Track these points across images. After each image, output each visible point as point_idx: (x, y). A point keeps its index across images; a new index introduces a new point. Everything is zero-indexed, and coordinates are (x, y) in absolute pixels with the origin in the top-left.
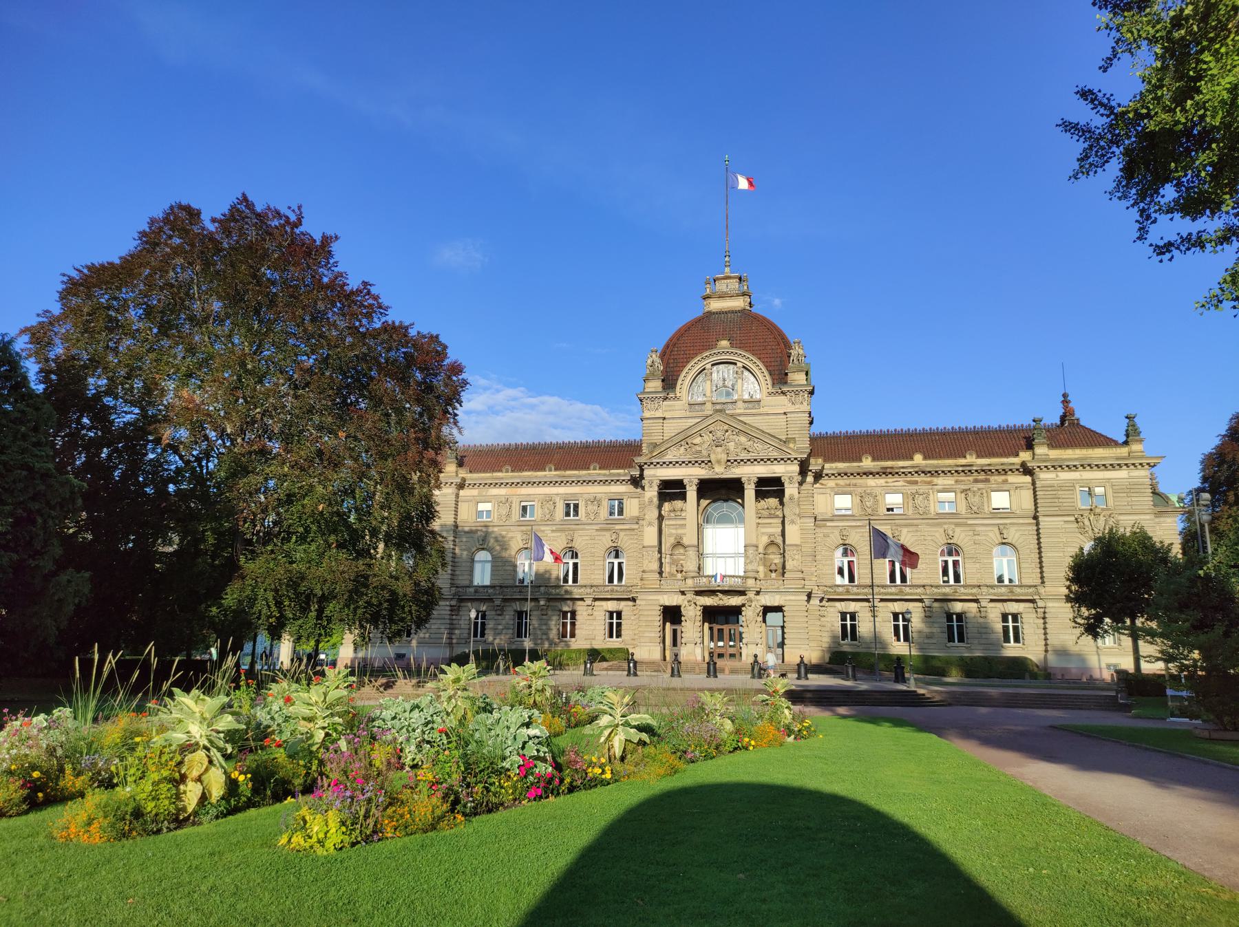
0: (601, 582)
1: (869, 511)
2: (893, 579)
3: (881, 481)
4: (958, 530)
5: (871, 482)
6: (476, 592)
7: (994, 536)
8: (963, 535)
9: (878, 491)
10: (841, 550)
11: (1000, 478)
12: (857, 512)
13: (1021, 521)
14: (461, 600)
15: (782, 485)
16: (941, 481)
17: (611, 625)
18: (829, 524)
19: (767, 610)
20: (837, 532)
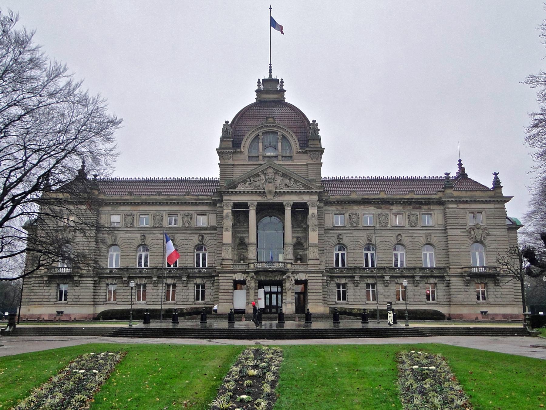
0: (191, 266)
1: (355, 225)
2: (367, 264)
3: (362, 207)
4: (403, 235)
5: (355, 208)
6: (111, 272)
7: (423, 240)
8: (406, 238)
9: (359, 212)
10: (337, 247)
11: (426, 207)
12: (348, 224)
13: (437, 231)
14: (100, 278)
15: (307, 207)
16: (394, 208)
17: (198, 293)
18: (331, 232)
19: (298, 282)
20: (336, 236)
